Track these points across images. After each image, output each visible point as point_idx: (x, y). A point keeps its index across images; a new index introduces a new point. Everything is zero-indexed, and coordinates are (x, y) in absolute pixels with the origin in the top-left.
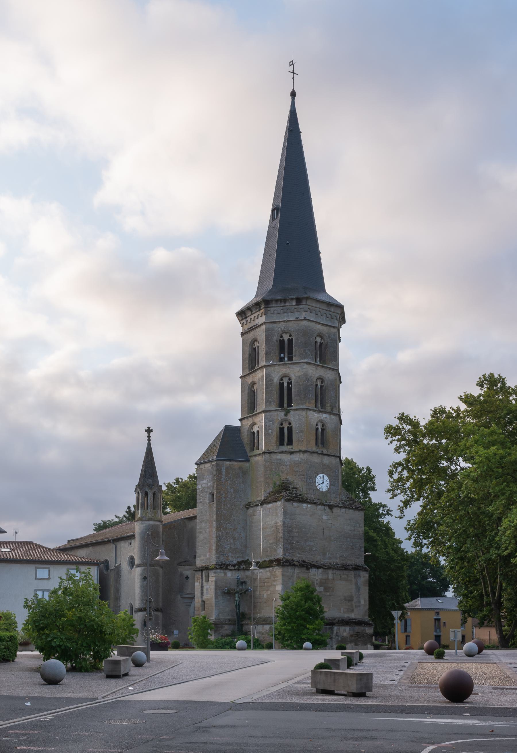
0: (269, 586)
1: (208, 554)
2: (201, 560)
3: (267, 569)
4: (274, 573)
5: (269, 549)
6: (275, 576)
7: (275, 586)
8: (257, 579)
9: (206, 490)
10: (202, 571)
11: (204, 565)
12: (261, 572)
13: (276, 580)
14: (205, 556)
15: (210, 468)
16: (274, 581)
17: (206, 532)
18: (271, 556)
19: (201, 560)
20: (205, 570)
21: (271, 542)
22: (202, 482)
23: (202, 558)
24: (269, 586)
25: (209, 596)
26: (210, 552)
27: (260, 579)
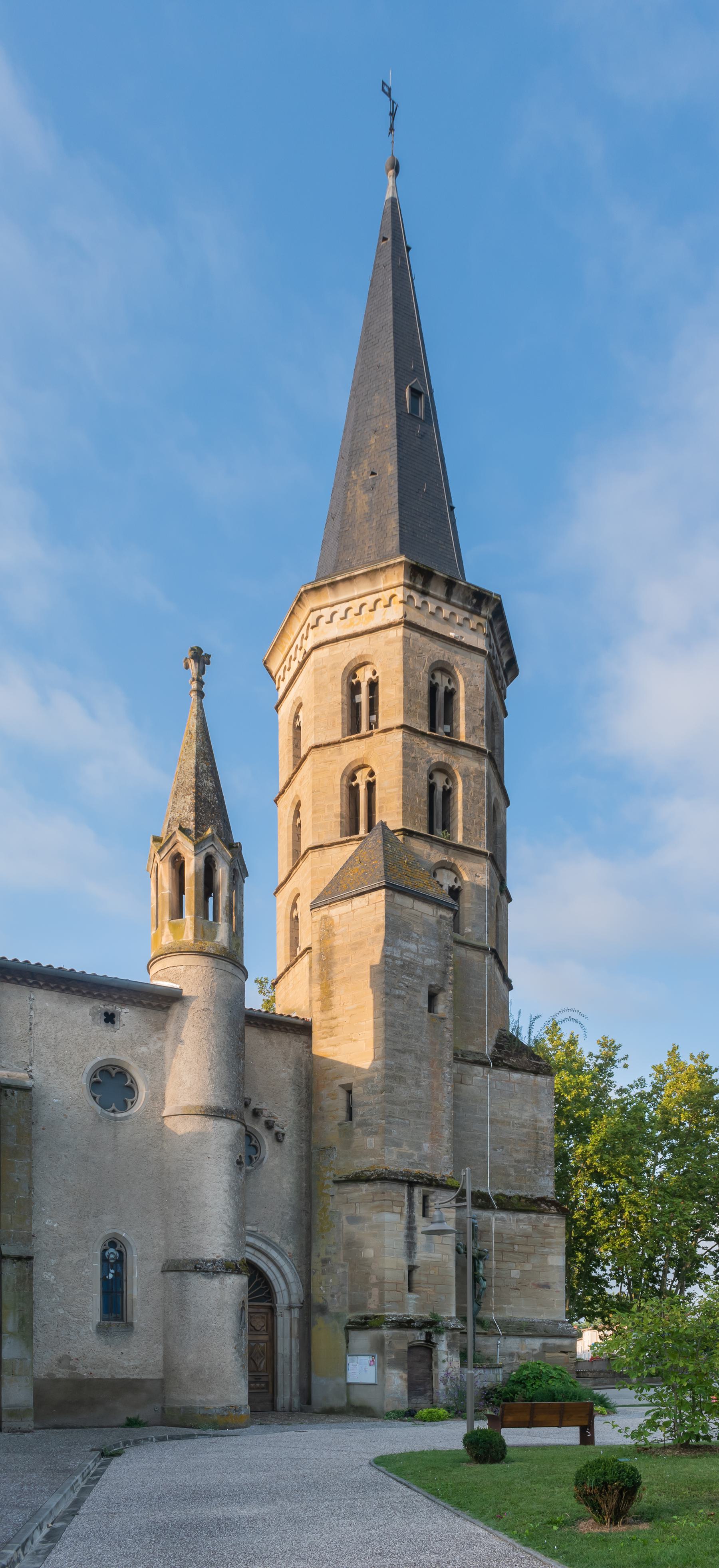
0: (529, 1254)
1: (426, 1147)
2: (401, 1155)
3: (522, 1216)
4: (541, 1227)
5: (512, 1171)
6: (545, 1234)
7: (544, 1256)
8: (489, 1231)
9: (419, 972)
10: (411, 1185)
11: (416, 1170)
12: (502, 1219)
13: (550, 1244)
14: (419, 1147)
15: (433, 920)
16: (543, 1245)
17: (418, 1085)
18: (520, 1188)
19: (401, 1155)
20: (421, 1184)
21: (520, 1156)
22: (405, 945)
23: (406, 1149)
24: (529, 1254)
25: (437, 1256)
26: (434, 1141)
27: (499, 1234)
